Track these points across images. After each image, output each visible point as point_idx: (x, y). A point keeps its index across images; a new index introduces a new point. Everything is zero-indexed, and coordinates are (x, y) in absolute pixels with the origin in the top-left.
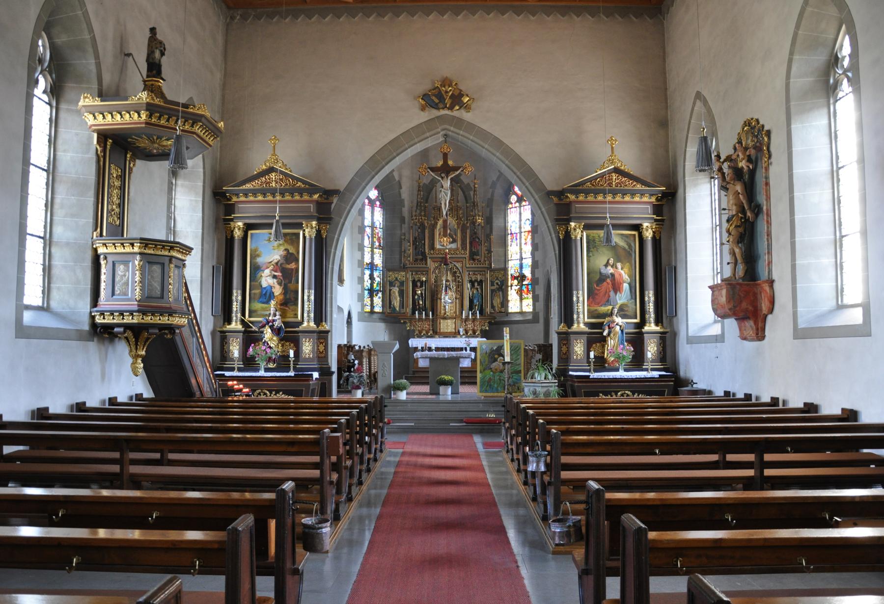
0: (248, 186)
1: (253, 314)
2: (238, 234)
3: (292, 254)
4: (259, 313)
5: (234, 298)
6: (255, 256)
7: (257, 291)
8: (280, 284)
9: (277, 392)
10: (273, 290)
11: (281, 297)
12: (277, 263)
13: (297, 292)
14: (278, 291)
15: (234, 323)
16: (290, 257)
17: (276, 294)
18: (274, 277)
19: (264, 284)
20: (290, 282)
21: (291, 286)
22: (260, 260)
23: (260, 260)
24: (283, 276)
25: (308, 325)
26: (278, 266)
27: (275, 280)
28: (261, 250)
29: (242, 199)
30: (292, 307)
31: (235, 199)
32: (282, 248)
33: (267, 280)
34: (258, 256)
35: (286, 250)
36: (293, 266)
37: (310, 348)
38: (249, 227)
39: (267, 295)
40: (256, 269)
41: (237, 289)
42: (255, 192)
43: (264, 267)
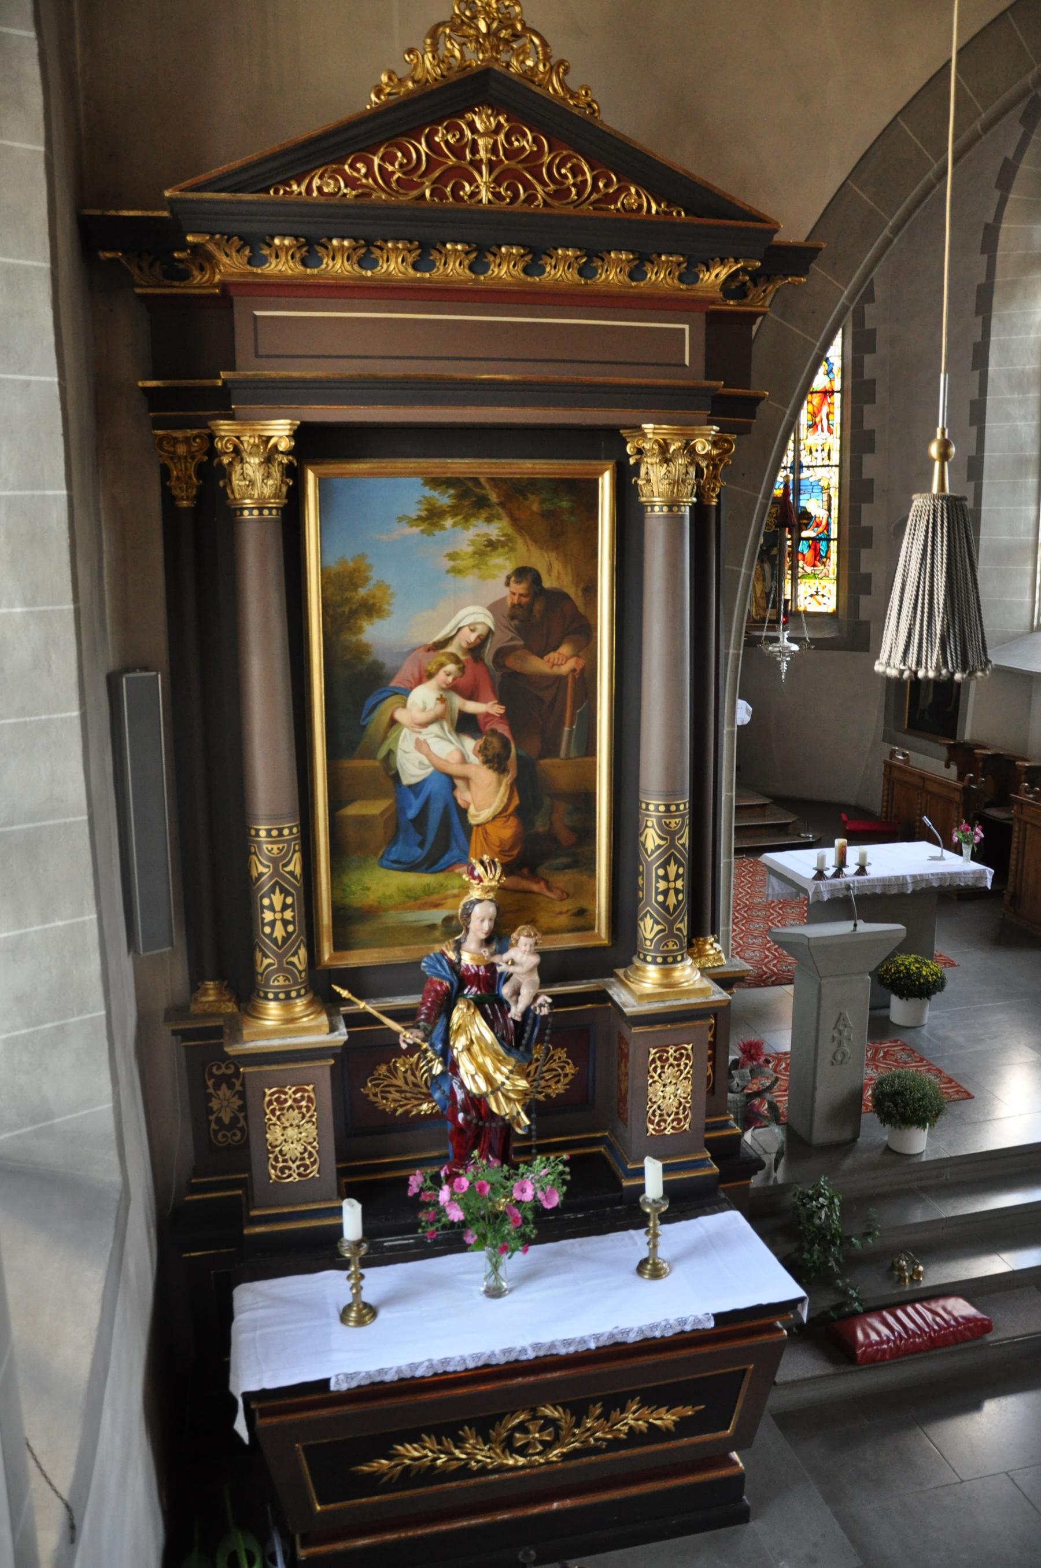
0: (323, 185)
1: (363, 930)
2: (254, 484)
3: (558, 597)
4: (392, 918)
5: (261, 868)
6: (348, 609)
7: (374, 808)
8: (496, 761)
9: (615, 1404)
10: (463, 796)
11: (506, 831)
12: (475, 650)
13: (590, 798)
14: (485, 797)
15: (273, 1010)
16: (546, 615)
17: (478, 815)
18: (466, 724)
19: (412, 767)
20: (550, 749)
21: (558, 770)
22: (378, 635)
23: (378, 635)
24: (507, 717)
25: (668, 983)
26: (486, 666)
27: (470, 744)
28: (382, 574)
29: (282, 267)
30: (563, 880)
31: (231, 264)
32: (503, 564)
33: (424, 741)
34: (371, 609)
35: (521, 573)
36: (562, 661)
37: (684, 1088)
38: (314, 444)
39: (433, 832)
40: (362, 687)
41: (275, 818)
42: (367, 225)
43: (407, 671)
